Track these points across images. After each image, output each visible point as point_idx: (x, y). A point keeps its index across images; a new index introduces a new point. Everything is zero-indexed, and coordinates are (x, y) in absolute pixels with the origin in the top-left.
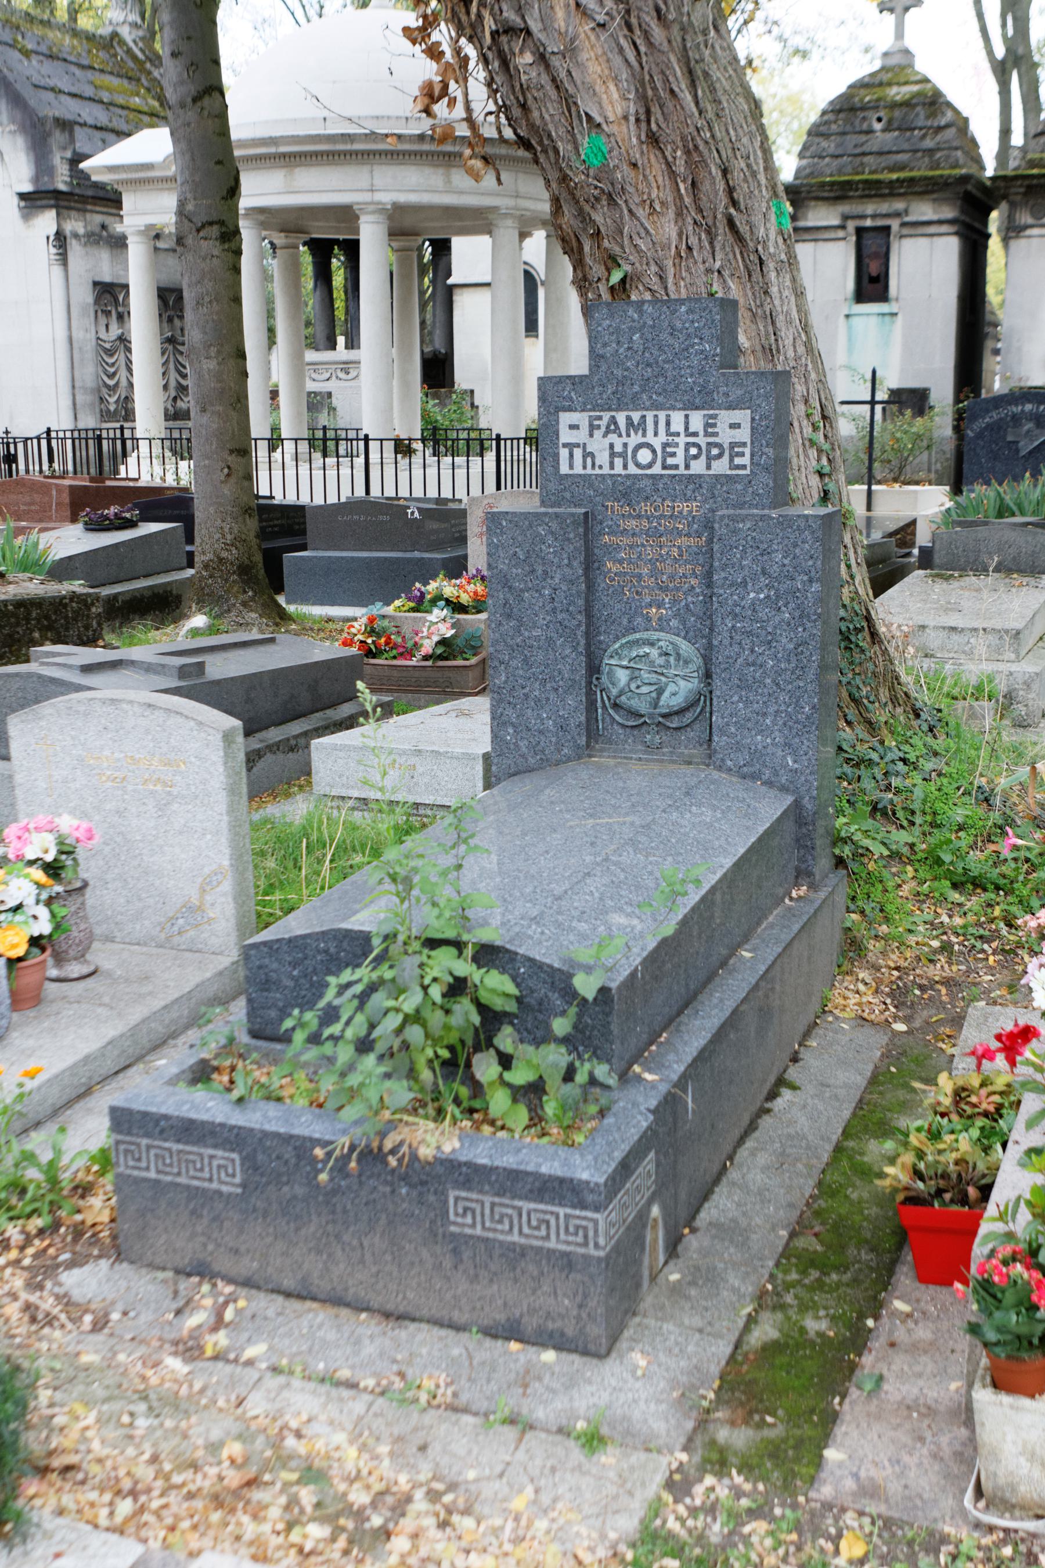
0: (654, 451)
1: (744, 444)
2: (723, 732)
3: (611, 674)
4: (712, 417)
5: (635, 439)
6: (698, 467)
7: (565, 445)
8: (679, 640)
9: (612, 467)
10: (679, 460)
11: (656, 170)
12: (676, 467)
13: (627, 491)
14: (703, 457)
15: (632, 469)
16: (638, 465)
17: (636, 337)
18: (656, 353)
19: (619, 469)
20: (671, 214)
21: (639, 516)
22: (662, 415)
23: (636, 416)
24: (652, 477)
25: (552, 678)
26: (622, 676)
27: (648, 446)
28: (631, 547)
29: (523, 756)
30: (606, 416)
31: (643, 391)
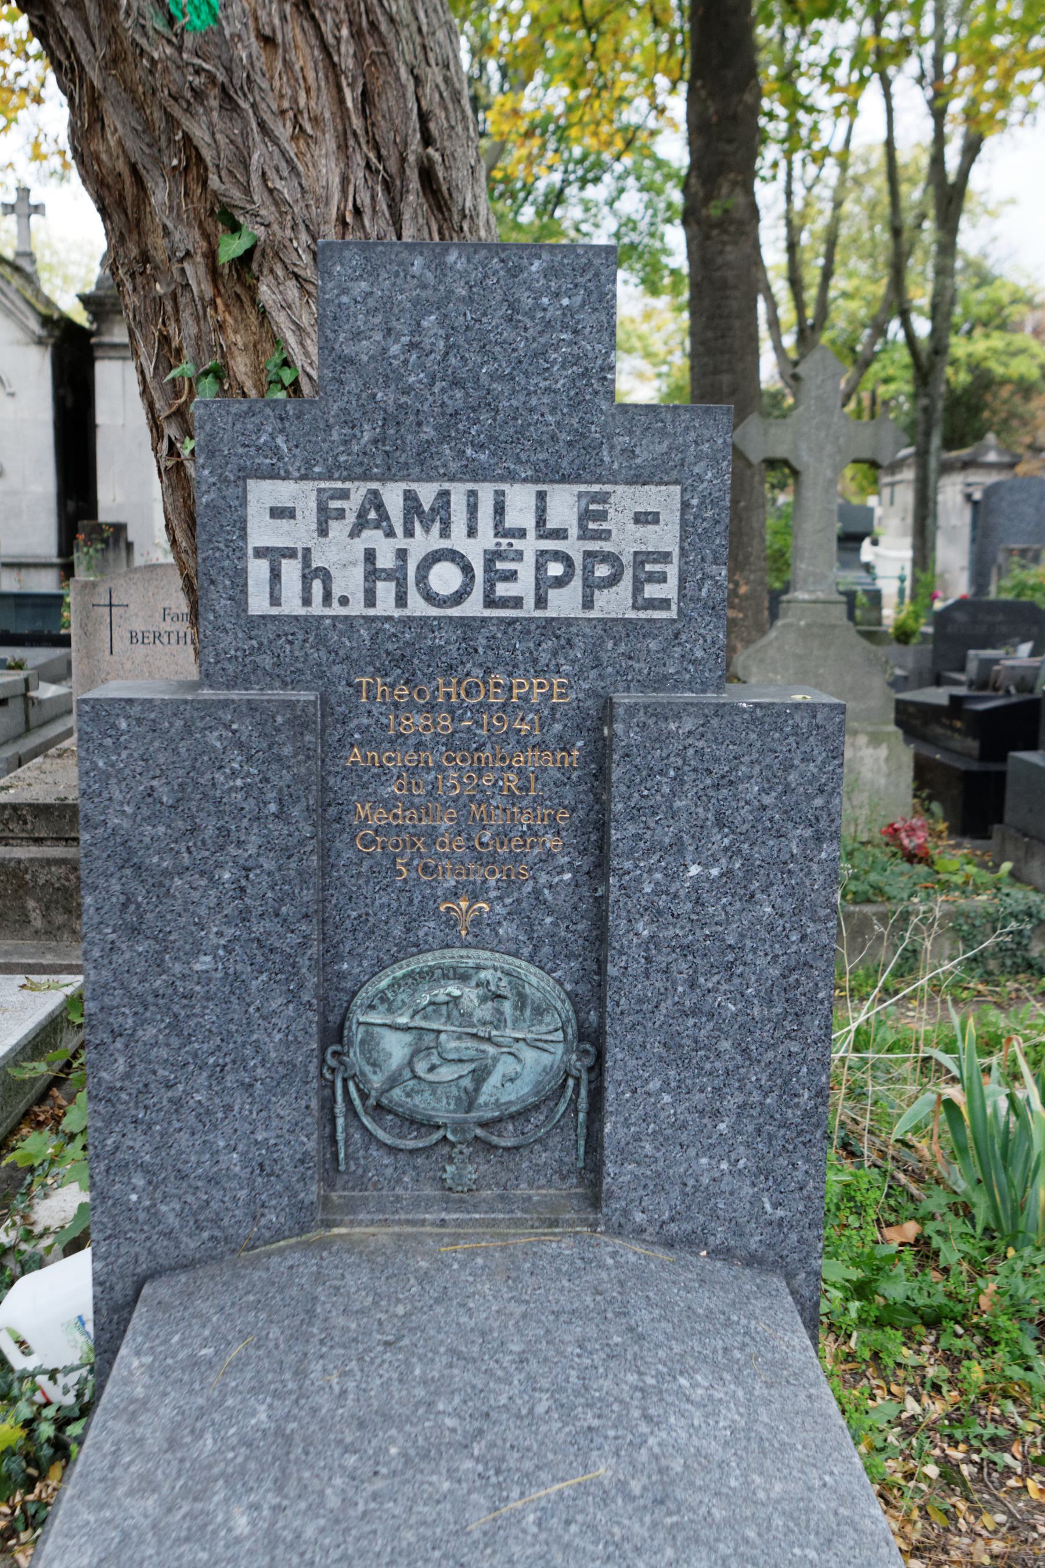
0: (467, 569)
1: (664, 557)
2: (624, 1155)
3: (369, 1043)
4: (595, 498)
5: (423, 542)
6: (565, 603)
7: (260, 553)
8: (522, 967)
9: (370, 599)
10: (524, 586)
11: (304, 56)
12: (517, 602)
13: (404, 652)
14: (577, 583)
15: (417, 606)
16: (430, 597)
17: (430, 321)
18: (474, 358)
19: (386, 604)
20: (330, 143)
21: (432, 707)
22: (486, 493)
23: (427, 493)
24: (464, 623)
25: (241, 1063)
26: (396, 1048)
27: (453, 556)
28: (413, 772)
29: (168, 1234)
30: (359, 491)
31: (446, 439)
